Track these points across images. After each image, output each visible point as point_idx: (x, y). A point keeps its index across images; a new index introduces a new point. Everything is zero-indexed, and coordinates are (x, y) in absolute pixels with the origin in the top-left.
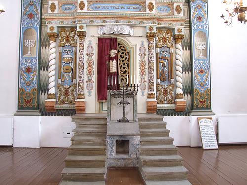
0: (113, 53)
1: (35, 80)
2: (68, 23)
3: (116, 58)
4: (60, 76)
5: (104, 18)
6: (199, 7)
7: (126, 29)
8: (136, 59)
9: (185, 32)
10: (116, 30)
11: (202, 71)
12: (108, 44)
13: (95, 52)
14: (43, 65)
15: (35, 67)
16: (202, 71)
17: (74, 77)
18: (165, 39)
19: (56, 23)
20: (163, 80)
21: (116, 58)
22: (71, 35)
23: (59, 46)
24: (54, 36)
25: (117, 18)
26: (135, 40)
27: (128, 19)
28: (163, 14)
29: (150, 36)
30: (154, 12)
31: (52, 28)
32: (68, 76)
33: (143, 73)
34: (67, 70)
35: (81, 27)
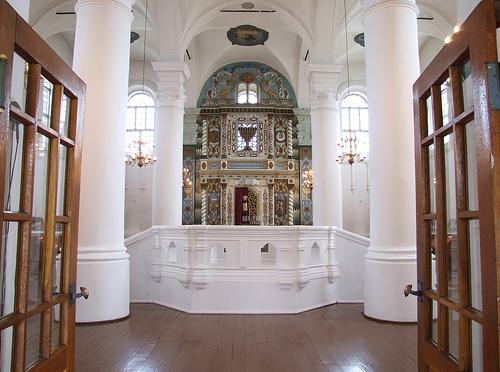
0: (245, 198)
1: (193, 215)
2: (215, 177)
3: (247, 201)
4: (209, 213)
5: (239, 174)
6: (306, 163)
7: (255, 182)
8: (261, 201)
9: (295, 181)
10: (248, 182)
11: (307, 209)
12: (242, 192)
13: (233, 197)
14: (198, 205)
15: (192, 207)
16: (307, 209)
17: (219, 214)
18: (281, 187)
19: (206, 177)
20: (279, 216)
21: (247, 201)
22: (215, 186)
23: (208, 192)
24: (204, 186)
25: (248, 174)
26: (259, 186)
27: (255, 175)
28: (280, 170)
29: (270, 186)
30: (273, 169)
31: (204, 181)
32: (214, 213)
33: (265, 211)
34: (214, 209)
35: (224, 180)
